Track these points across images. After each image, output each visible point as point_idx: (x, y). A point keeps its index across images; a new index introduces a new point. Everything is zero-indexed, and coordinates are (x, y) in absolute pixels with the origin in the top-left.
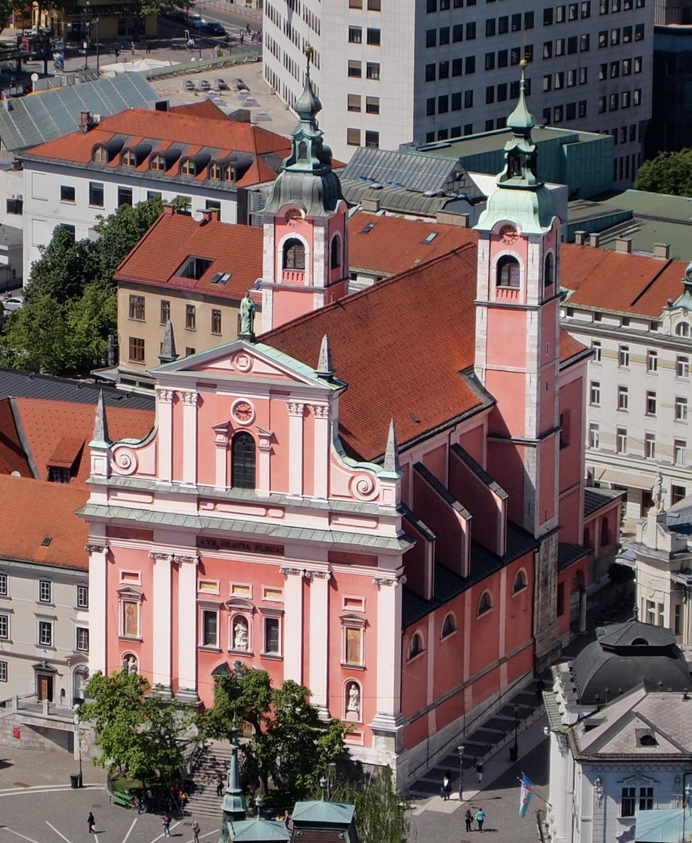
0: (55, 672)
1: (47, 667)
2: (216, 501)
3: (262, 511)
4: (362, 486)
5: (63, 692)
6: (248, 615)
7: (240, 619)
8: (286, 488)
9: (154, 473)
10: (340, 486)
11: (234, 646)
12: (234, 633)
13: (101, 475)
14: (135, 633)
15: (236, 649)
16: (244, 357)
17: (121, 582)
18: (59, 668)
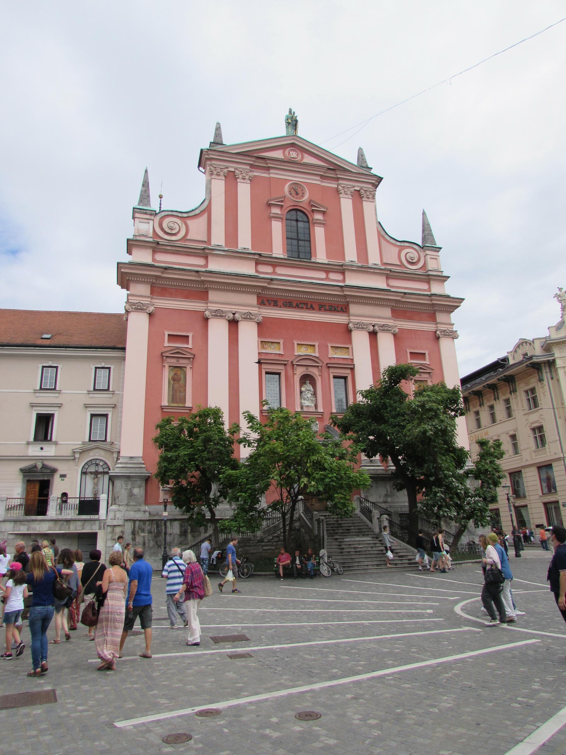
0: (54, 471)
1: (44, 467)
2: (275, 263)
3: (323, 275)
4: (412, 256)
5: (65, 495)
6: (314, 372)
7: (307, 379)
8: (343, 255)
9: (205, 239)
10: (392, 256)
11: (302, 408)
12: (301, 392)
13: (146, 236)
14: (184, 402)
15: (305, 409)
16: (294, 151)
17: (166, 344)
18: (62, 468)
